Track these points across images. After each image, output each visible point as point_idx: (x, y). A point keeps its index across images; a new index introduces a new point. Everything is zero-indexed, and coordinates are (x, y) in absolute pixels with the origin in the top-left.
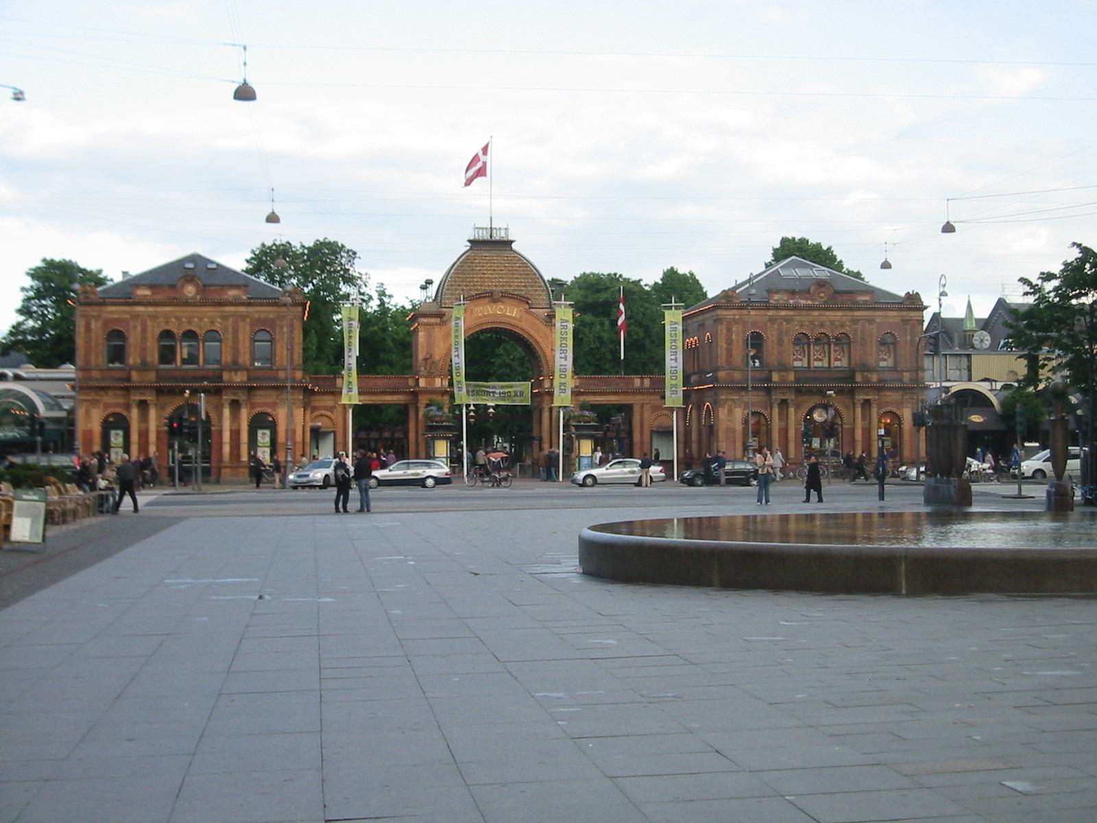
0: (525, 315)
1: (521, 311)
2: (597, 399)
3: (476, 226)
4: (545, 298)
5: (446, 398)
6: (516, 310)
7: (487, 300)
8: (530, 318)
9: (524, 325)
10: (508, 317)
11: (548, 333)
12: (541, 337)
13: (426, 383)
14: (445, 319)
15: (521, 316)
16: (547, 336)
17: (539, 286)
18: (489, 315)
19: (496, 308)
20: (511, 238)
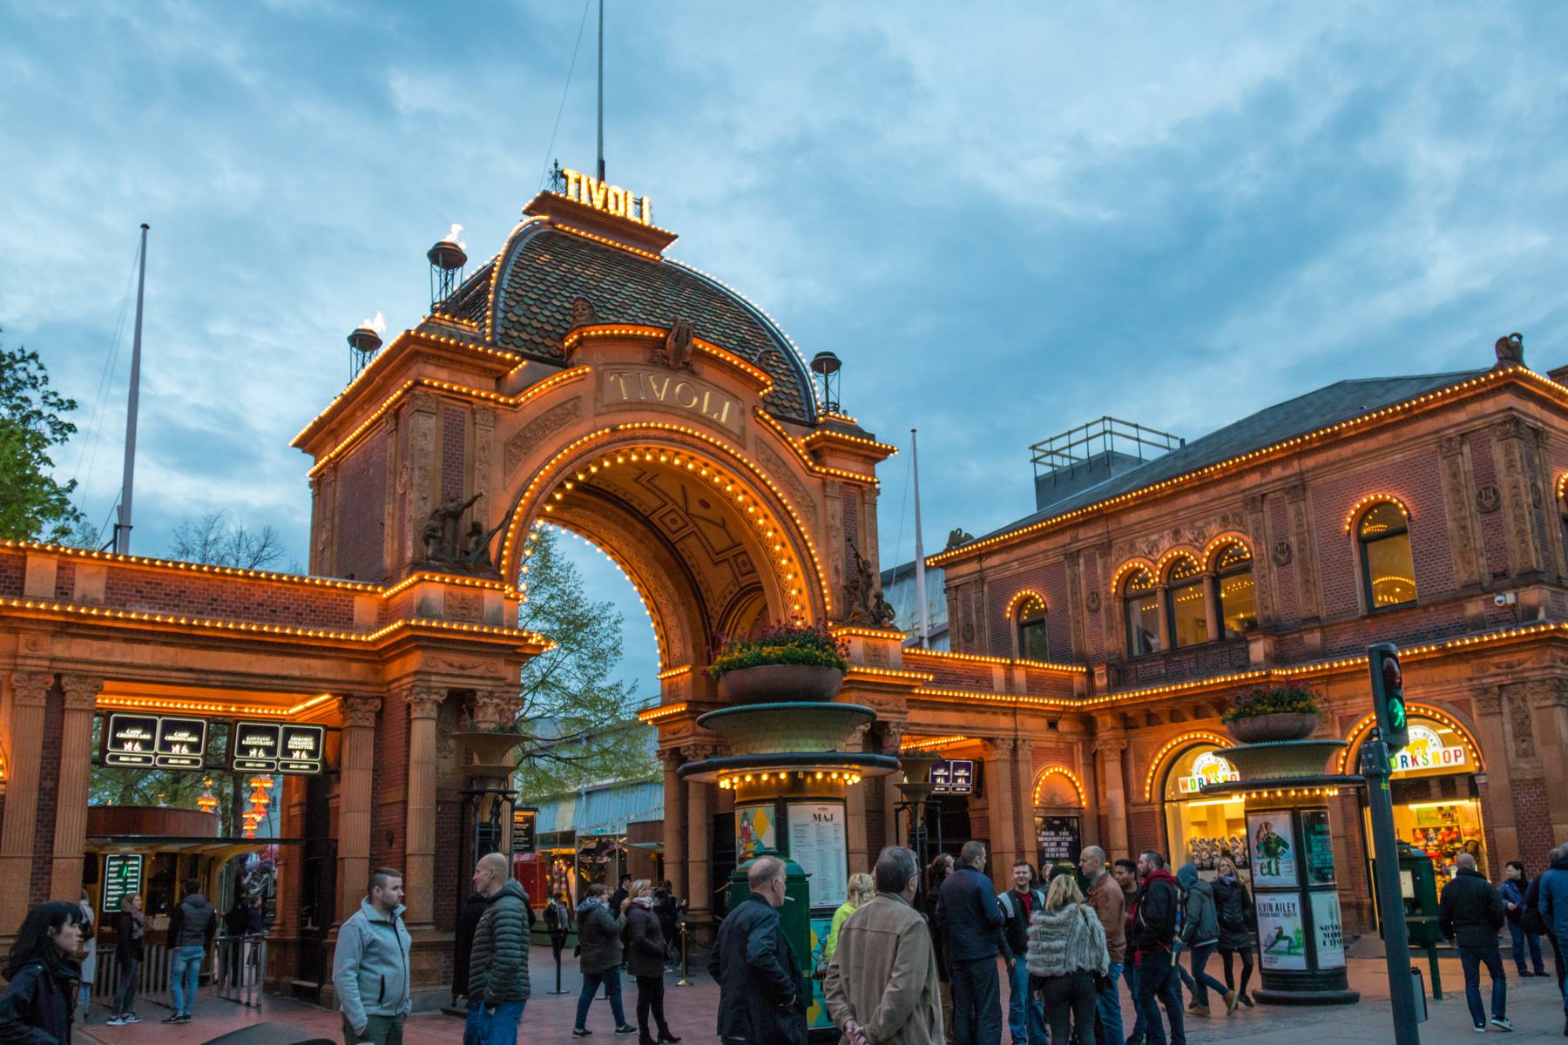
1: (743, 413)
3: (560, 167)
6: (727, 405)
15: (743, 428)
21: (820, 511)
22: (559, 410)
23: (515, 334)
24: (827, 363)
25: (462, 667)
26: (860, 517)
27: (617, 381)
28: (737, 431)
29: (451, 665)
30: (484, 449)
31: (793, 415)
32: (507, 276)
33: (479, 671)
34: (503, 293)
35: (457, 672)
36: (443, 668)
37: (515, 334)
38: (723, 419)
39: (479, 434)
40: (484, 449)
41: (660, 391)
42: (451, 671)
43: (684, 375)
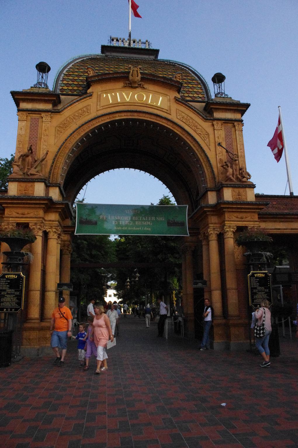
0: (175, 106)
2: (278, 227)
4: (200, 91)
5: (53, 217)
7: (120, 85)
8: (182, 108)
9: (173, 117)
10: (152, 107)
11: (210, 130)
12: (199, 134)
13: (19, 190)
14: (60, 107)
16: (208, 134)
17: (193, 80)
18: (124, 104)
19: (133, 96)
20: (153, 47)
21: (211, 136)
22: (80, 111)
23: (66, 88)
24: (219, 78)
25: (23, 214)
26: (234, 137)
27: (107, 97)
28: (167, 109)
29: (18, 213)
30: (46, 130)
31: (200, 100)
32: (66, 69)
33: (32, 215)
34: (63, 75)
35: (21, 216)
36: (15, 215)
37: (66, 88)
38: (159, 104)
39: (44, 124)
40: (46, 130)
41: (128, 98)
42: (18, 215)
43: (139, 90)
